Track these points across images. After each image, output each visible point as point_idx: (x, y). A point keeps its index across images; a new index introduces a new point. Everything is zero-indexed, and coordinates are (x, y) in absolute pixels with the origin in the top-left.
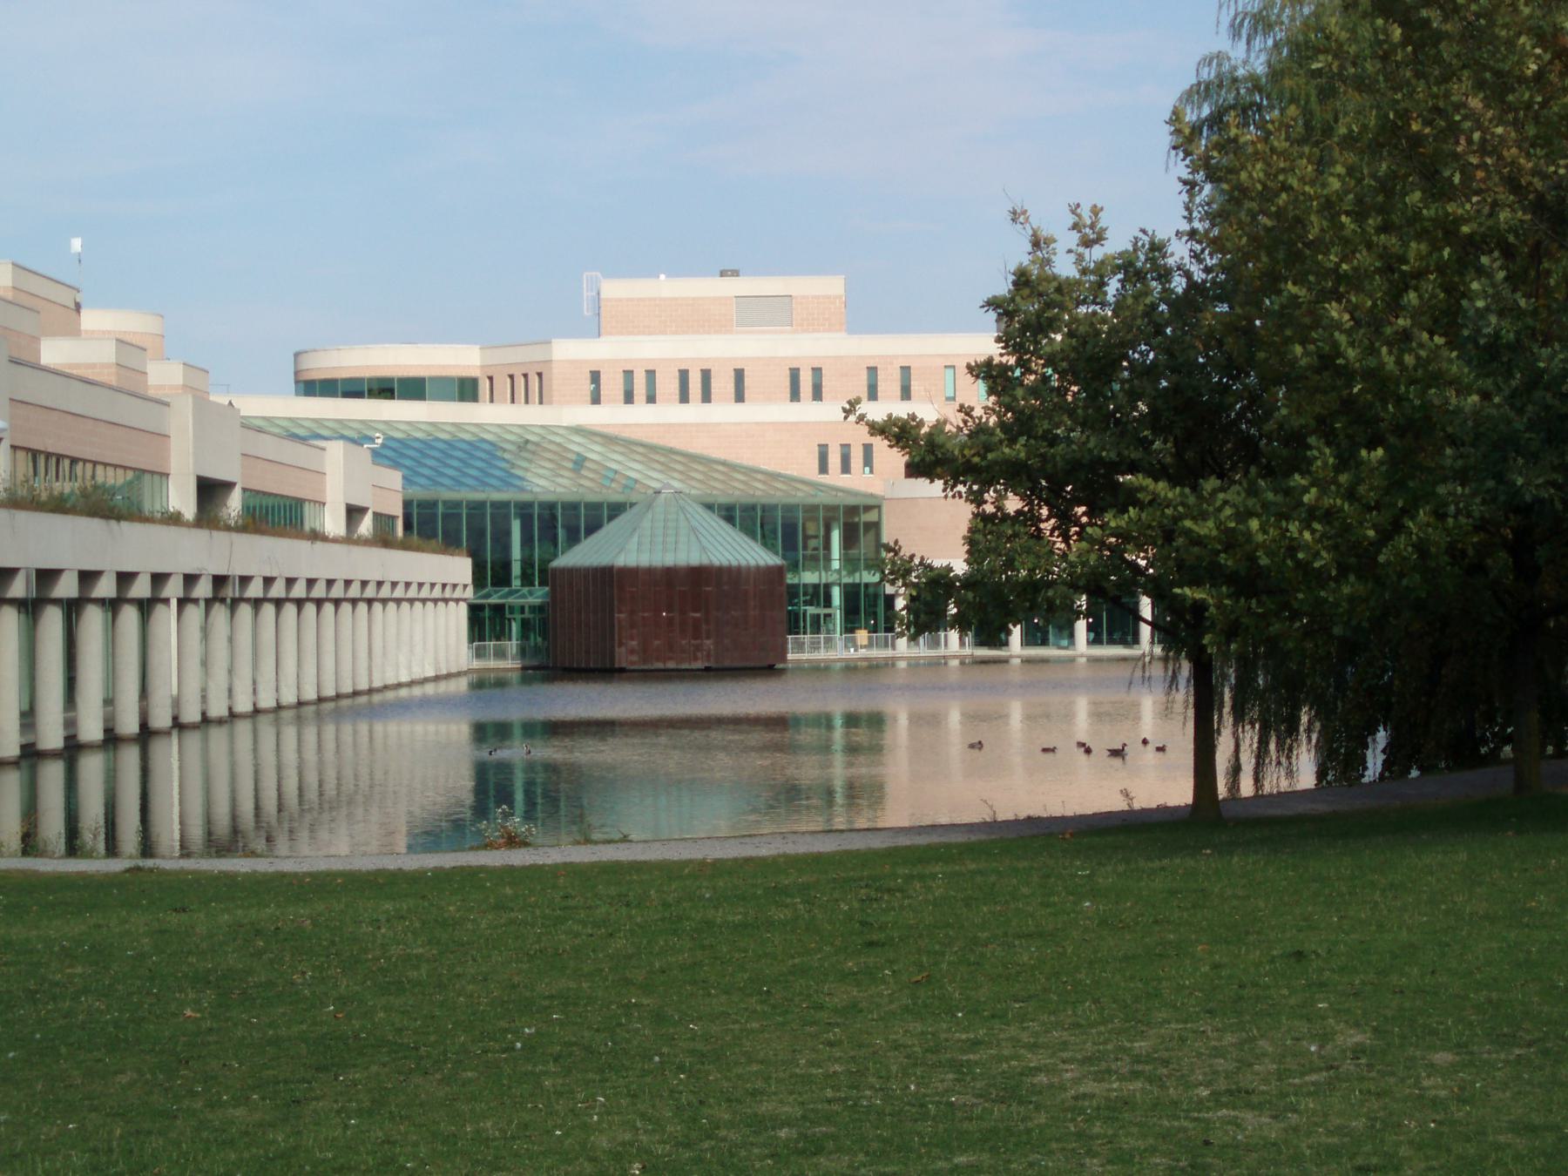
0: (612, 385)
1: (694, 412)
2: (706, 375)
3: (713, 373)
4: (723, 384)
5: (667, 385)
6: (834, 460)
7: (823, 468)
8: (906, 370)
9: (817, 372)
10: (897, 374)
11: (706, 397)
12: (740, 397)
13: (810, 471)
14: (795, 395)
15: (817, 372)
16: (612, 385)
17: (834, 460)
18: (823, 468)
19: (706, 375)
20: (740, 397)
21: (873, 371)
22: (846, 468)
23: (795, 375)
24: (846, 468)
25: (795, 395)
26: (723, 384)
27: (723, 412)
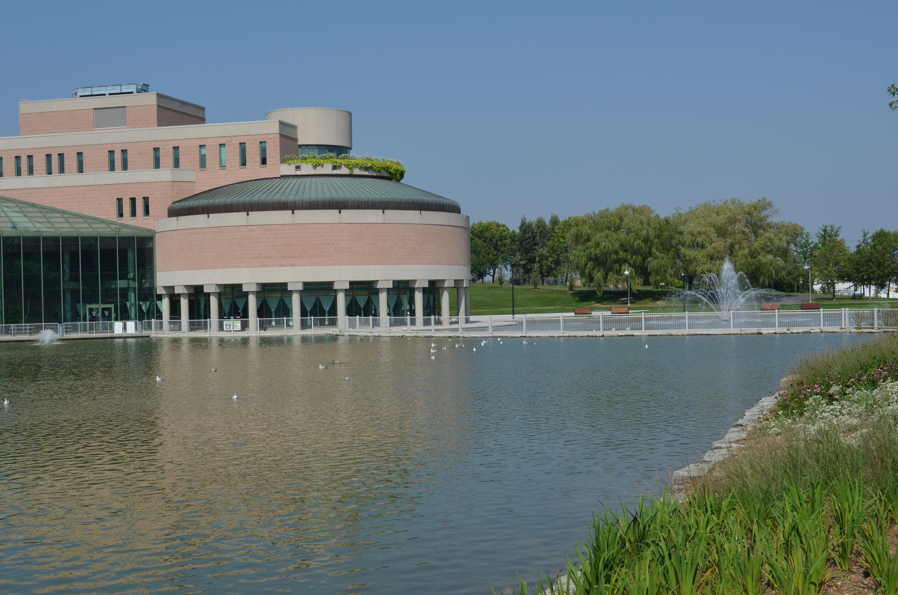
1: (57, 180)
2: (61, 156)
3: (65, 156)
4: (71, 162)
5: (40, 163)
7: (121, 215)
10: (171, 152)
11: (62, 170)
12: (81, 170)
13: (111, 214)
14: (112, 168)
18: (121, 215)
19: (61, 156)
20: (81, 170)
21: (156, 150)
22: (134, 213)
24: (134, 213)
25: (112, 168)
26: (71, 162)
27: (71, 179)
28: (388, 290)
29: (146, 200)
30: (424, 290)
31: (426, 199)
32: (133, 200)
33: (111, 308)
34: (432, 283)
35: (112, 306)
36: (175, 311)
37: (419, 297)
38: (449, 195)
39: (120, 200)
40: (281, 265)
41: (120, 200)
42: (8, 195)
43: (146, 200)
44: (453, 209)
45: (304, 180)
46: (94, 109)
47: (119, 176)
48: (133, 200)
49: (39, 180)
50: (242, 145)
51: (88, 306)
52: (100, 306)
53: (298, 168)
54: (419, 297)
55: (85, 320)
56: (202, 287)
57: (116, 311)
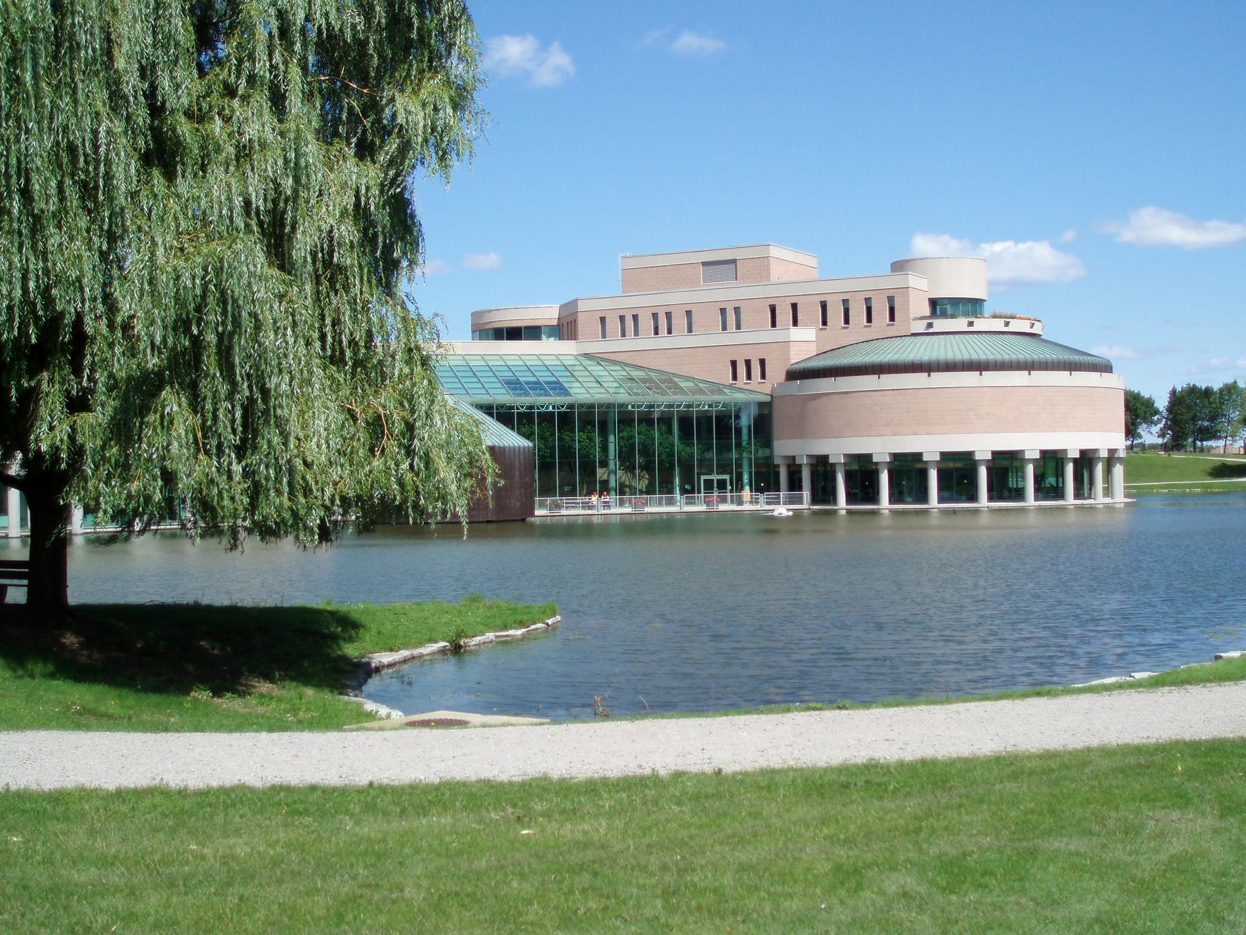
0: (613, 325)
1: (664, 341)
4: (680, 322)
5: (646, 323)
6: (741, 370)
7: (735, 377)
8: (794, 307)
9: (737, 310)
15: (737, 310)
16: (613, 325)
17: (741, 370)
18: (735, 377)
19: (669, 316)
22: (749, 377)
23: (723, 311)
24: (749, 377)
26: (680, 322)
27: (681, 340)
28: (1034, 460)
29: (762, 362)
30: (1075, 461)
31: (1077, 358)
32: (748, 363)
33: (725, 480)
34: (1083, 452)
35: (727, 477)
36: (795, 484)
37: (1070, 469)
38: (1101, 351)
39: (734, 364)
40: (915, 434)
41: (734, 364)
42: (612, 357)
43: (762, 362)
44: (1106, 368)
45: (934, 338)
46: (704, 264)
47: (731, 337)
48: (748, 363)
49: (647, 342)
50: (868, 300)
51: (703, 478)
52: (715, 477)
53: (930, 325)
54: (1070, 469)
55: (699, 492)
56: (826, 457)
57: (731, 485)
